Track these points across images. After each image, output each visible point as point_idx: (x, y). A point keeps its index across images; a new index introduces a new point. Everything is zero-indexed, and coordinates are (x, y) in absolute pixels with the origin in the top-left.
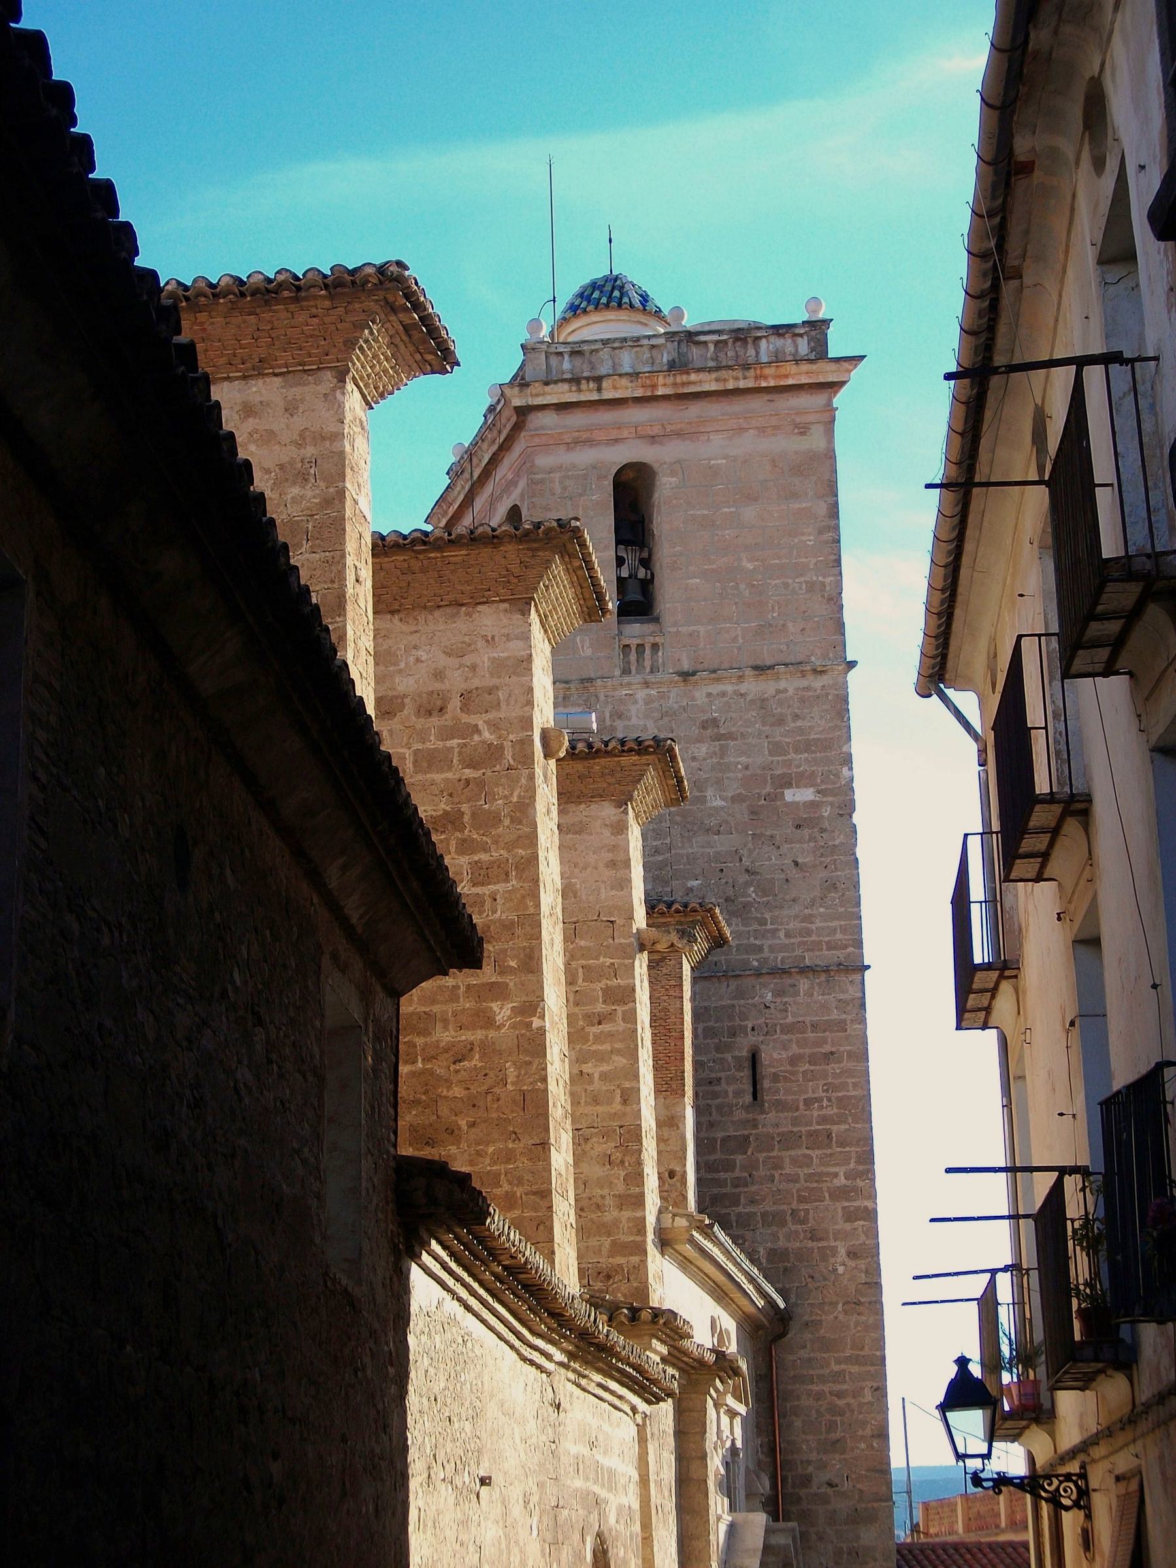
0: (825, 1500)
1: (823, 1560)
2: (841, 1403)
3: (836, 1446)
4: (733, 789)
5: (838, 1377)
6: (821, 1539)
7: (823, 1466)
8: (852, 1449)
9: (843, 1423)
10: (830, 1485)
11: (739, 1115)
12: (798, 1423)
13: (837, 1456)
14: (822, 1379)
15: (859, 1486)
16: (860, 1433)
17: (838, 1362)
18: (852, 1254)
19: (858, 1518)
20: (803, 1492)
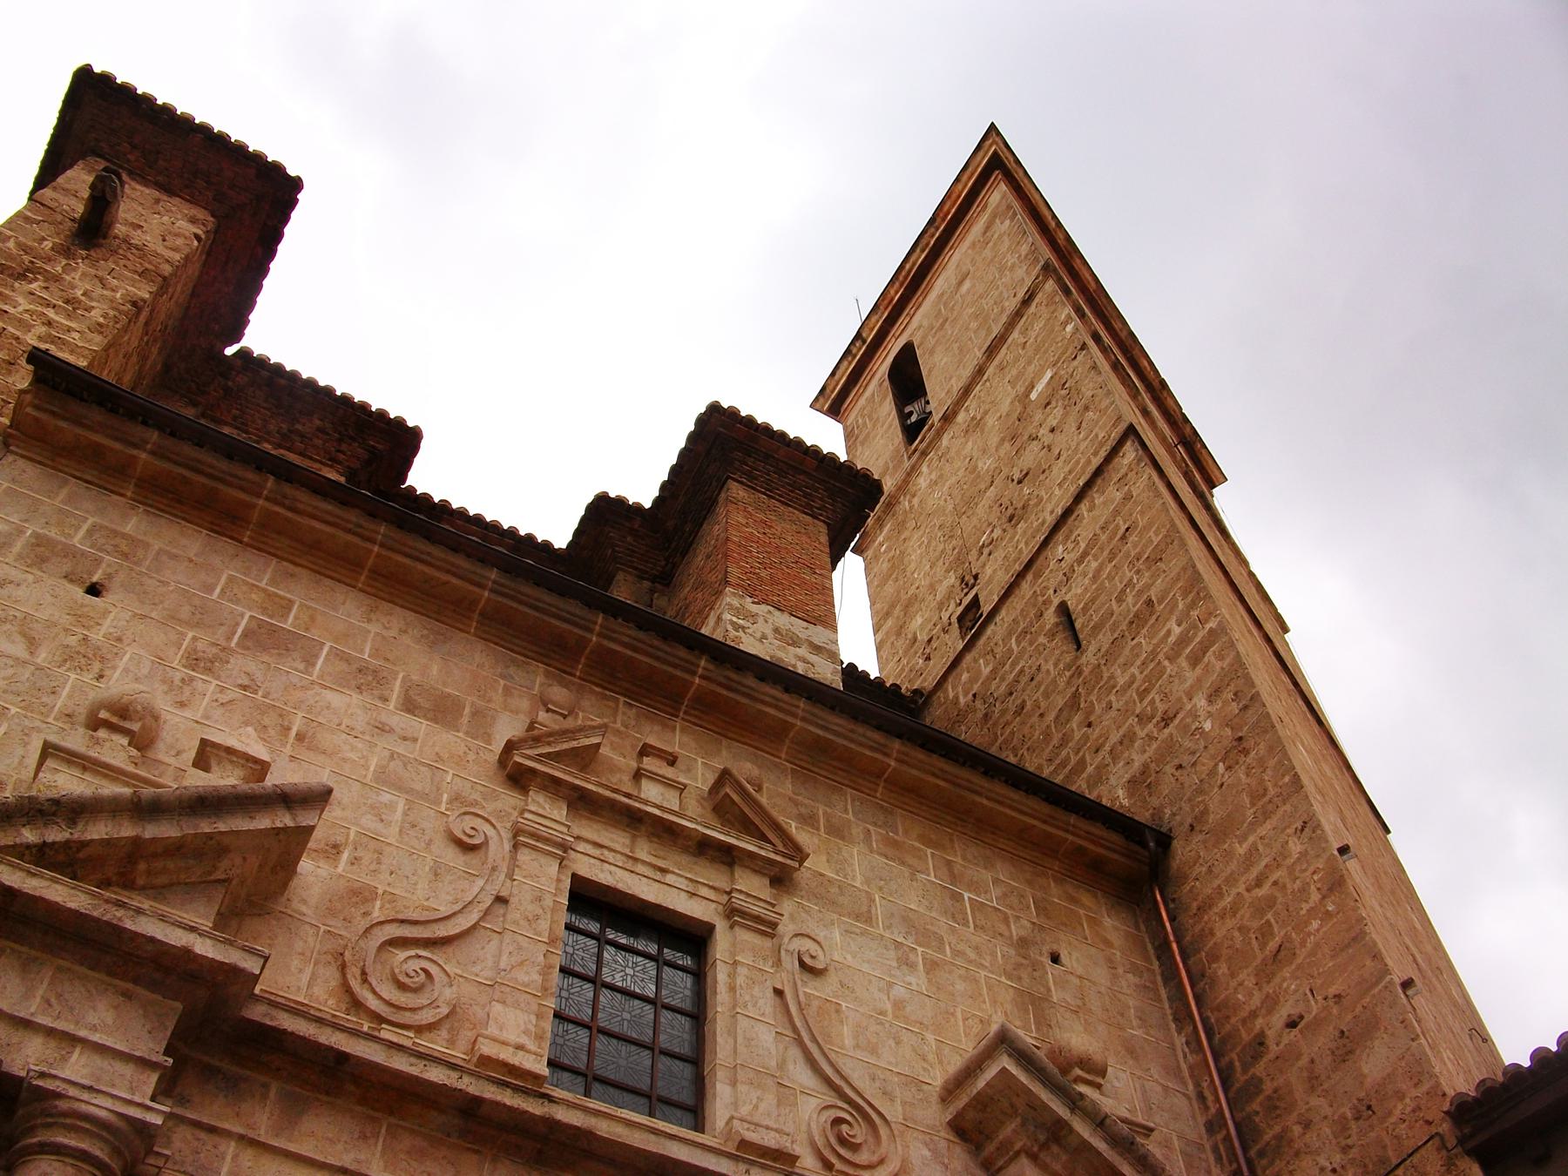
0: (1292, 1054)
1: (1323, 1162)
3: (1279, 956)
4: (994, 440)
5: (1251, 856)
6: (1307, 1125)
7: (1271, 1003)
8: (1303, 943)
9: (1277, 914)
10: (1292, 1024)
13: (1286, 972)
14: (1231, 880)
15: (1332, 991)
16: (1305, 907)
19: (1347, 1047)
20: (1259, 1069)
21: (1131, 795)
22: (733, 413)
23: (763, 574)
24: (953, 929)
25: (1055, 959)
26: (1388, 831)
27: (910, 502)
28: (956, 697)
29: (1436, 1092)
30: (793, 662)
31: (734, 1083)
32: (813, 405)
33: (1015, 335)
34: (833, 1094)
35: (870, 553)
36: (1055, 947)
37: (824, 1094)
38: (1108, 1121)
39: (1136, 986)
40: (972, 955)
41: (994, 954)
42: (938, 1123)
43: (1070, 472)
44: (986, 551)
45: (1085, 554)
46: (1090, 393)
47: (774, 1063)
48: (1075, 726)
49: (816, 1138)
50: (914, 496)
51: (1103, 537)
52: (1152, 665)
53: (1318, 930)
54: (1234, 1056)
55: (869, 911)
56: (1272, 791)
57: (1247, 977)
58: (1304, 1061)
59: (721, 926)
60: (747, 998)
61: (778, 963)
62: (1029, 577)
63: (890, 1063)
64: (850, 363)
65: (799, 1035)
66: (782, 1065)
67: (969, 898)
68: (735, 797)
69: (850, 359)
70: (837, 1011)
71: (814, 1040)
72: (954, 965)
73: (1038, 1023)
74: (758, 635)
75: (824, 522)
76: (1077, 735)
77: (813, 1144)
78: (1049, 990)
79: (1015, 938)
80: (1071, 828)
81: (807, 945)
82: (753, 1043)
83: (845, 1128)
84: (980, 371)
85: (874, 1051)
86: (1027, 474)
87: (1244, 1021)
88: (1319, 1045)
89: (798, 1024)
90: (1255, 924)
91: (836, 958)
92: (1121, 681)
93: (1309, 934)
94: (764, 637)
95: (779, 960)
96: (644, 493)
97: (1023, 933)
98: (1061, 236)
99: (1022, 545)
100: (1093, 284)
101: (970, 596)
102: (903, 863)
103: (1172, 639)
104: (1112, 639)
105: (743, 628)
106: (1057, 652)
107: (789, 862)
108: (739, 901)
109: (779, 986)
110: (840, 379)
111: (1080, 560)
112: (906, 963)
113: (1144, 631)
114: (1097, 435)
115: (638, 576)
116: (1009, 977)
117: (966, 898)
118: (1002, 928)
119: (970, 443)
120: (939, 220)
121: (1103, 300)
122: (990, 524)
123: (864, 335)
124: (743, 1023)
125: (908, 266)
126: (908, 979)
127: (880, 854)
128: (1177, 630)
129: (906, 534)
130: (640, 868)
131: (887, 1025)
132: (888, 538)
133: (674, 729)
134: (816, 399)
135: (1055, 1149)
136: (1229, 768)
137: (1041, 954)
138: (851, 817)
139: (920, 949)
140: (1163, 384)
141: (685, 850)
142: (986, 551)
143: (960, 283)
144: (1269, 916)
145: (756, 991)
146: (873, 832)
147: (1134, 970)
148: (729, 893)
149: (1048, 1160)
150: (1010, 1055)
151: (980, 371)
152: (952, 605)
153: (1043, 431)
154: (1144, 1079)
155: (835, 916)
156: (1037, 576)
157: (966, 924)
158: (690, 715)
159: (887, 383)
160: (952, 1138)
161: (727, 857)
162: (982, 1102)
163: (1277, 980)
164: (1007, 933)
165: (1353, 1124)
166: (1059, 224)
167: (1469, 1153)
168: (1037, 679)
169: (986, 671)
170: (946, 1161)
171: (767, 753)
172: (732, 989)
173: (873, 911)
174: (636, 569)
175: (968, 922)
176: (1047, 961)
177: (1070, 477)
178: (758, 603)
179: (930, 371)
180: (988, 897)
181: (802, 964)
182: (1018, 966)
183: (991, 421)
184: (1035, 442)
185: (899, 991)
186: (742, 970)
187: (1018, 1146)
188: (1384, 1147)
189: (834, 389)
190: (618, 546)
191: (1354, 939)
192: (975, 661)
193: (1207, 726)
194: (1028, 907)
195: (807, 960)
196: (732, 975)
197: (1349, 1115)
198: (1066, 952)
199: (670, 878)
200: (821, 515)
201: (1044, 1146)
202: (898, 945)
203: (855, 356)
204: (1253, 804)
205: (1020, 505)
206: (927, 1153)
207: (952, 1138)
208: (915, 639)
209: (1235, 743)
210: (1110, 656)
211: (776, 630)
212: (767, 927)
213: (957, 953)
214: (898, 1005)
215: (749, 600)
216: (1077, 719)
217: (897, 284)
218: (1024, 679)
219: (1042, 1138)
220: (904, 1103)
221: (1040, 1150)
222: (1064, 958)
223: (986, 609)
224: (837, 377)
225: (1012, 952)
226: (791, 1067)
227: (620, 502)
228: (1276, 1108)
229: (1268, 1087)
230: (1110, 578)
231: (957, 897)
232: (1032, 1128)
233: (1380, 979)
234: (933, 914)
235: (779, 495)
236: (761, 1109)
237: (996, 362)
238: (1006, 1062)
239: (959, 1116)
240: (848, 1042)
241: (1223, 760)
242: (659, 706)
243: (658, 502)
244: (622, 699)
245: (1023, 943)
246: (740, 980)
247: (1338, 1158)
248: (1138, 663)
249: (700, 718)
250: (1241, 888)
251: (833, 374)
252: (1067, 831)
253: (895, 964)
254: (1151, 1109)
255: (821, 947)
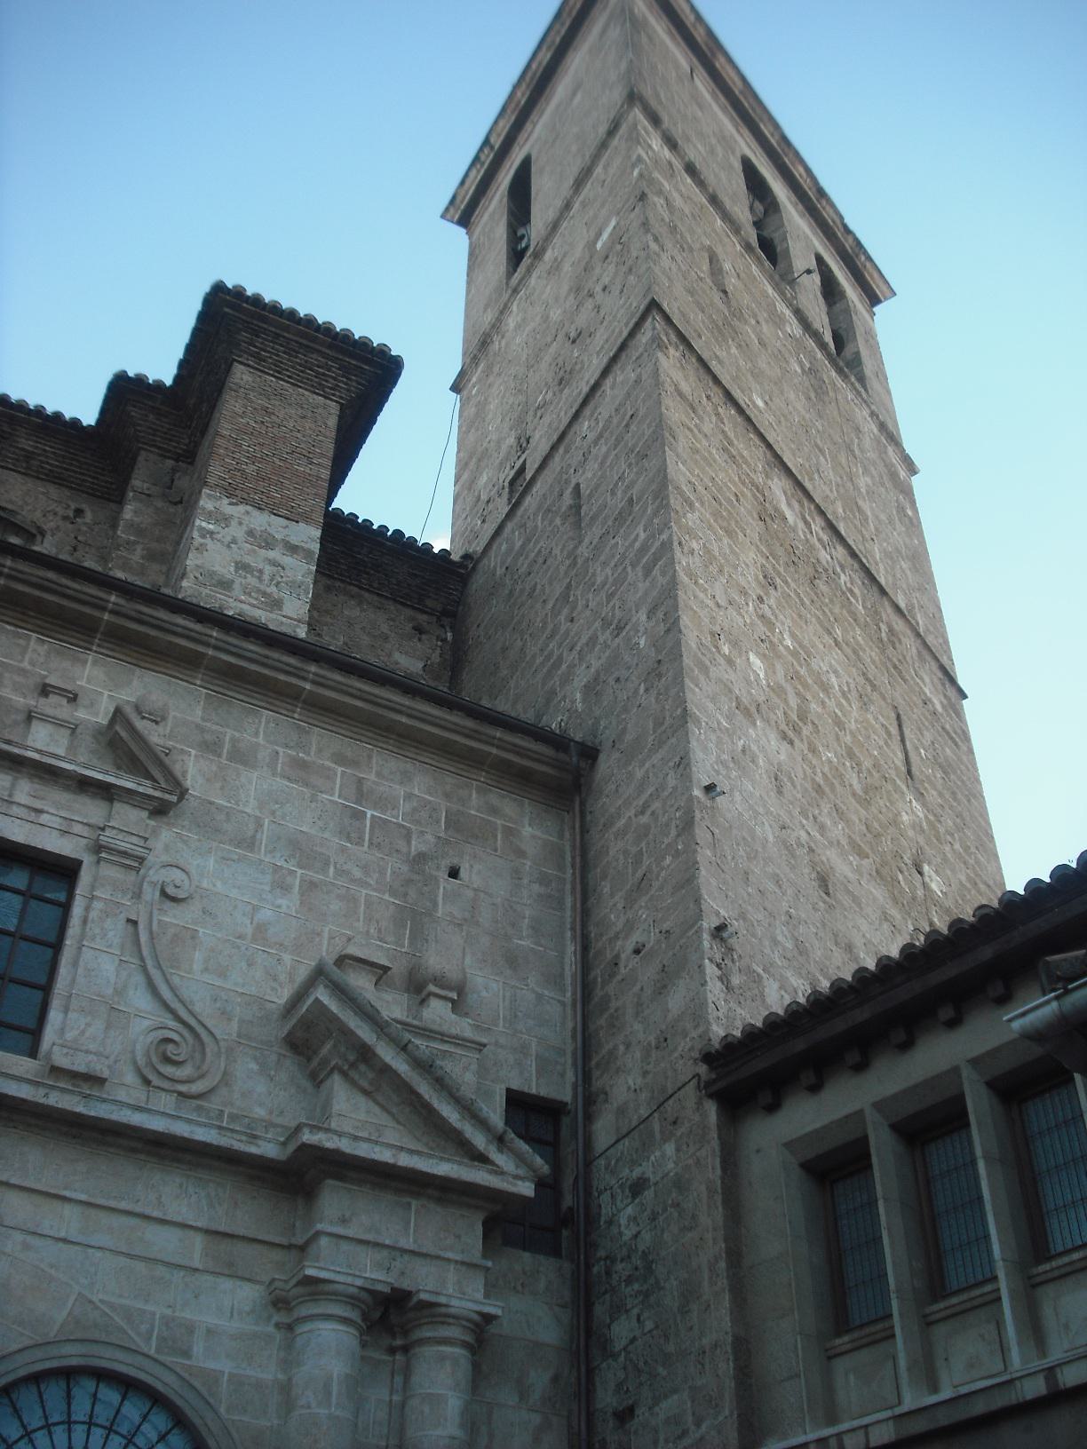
2: (644, 819)
4: (565, 288)
7: (630, 926)
8: (657, 879)
11: (563, 569)
12: (607, 890)
15: (666, 926)
16: (666, 841)
17: (642, 764)
18: (651, 614)
20: (611, 989)
21: (584, 701)
22: (239, 293)
23: (250, 469)
24: (343, 850)
25: (454, 873)
26: (965, 696)
27: (500, 342)
28: (495, 568)
29: (705, 1036)
30: (261, 567)
31: (66, 1010)
32: (443, 216)
33: (599, 170)
34: (170, 1016)
35: (465, 393)
36: (455, 861)
37: (159, 1016)
38: (410, 1046)
39: (540, 895)
40: (357, 873)
41: (382, 872)
42: (273, 1039)
43: (607, 341)
44: (539, 415)
45: (600, 436)
46: (635, 254)
47: (110, 991)
48: (563, 618)
49: (138, 1058)
50: (503, 337)
51: (615, 421)
52: (620, 570)
53: (669, 866)
54: (599, 971)
55: (254, 837)
56: (668, 721)
57: (619, 899)
58: (637, 988)
59: (87, 860)
60: (97, 931)
61: (138, 895)
62: (561, 450)
63: (236, 984)
64: (478, 171)
65: (144, 962)
66: (120, 992)
67: (373, 816)
68: (123, 734)
69: (478, 166)
70: (193, 938)
71: (159, 967)
72: (333, 884)
73: (413, 938)
74: (229, 539)
75: (336, 402)
76: (563, 628)
77: (135, 1063)
78: (435, 904)
79: (413, 852)
80: (496, 742)
81: (177, 875)
82: (93, 973)
83: (170, 1048)
84: (567, 206)
85: (223, 974)
86: (580, 333)
87: (610, 940)
88: (648, 974)
89: (146, 952)
90: (634, 850)
91: (205, 885)
92: (599, 580)
93: (662, 869)
94: (234, 541)
95: (141, 892)
96: (162, 367)
97: (423, 848)
98: (702, 31)
99: (562, 413)
100: (739, 83)
101: (521, 460)
102: (307, 785)
103: (637, 545)
104: (601, 532)
105: (212, 533)
106: (565, 537)
107: (167, 796)
108: (107, 837)
109: (134, 918)
110: (469, 188)
111: (596, 442)
112: (282, 887)
113: (622, 531)
114: (631, 304)
115: (161, 455)
116: (393, 893)
117: (369, 816)
118: (401, 844)
119: (549, 287)
120: (565, 15)
121: (751, 100)
122: (546, 384)
123: (492, 140)
124: (87, 954)
125: (534, 66)
126: (279, 901)
127: (283, 777)
128: (642, 536)
129: (491, 379)
130: (15, 810)
131: (243, 948)
132: (479, 380)
133: (86, 662)
134: (447, 209)
135: (363, 1067)
136: (647, 690)
137: (438, 868)
138: (261, 740)
139: (300, 871)
140: (821, 193)
141: (67, 788)
142: (539, 415)
143: (574, 94)
144: (643, 844)
145: (109, 923)
146: (281, 754)
147: (543, 880)
148: (103, 829)
149: (356, 1077)
150: (326, 986)
151: (567, 206)
152: (508, 468)
153: (598, 289)
154: (517, 988)
155: (215, 844)
156: (567, 451)
157: (360, 842)
158: (103, 647)
159: (505, 200)
160: (284, 1052)
161: (106, 792)
162: (306, 1024)
163: (636, 907)
164: (405, 850)
165: (654, 1053)
166: (699, 18)
167: (710, 1096)
168: (548, 563)
169: (518, 544)
170: (273, 1073)
171: (181, 680)
172: (85, 921)
173: (258, 836)
174: (159, 448)
175: (364, 840)
176: (443, 875)
177: (606, 346)
178: (236, 504)
179: (537, 194)
180: (395, 812)
181: (164, 894)
182: (409, 882)
183: (567, 267)
184: (590, 300)
185: (266, 914)
186: (97, 905)
187: (333, 1063)
188: (667, 1078)
189: (464, 197)
190: (140, 425)
191: (688, 880)
192: (513, 532)
193: (642, 642)
194: (438, 821)
195: (170, 891)
196: (87, 909)
197: (653, 1044)
198: (467, 866)
199: (44, 818)
200: (334, 395)
201: (353, 1065)
202: (277, 869)
203: (483, 164)
204: (654, 732)
205: (568, 370)
206: (254, 1066)
207: (284, 1052)
208: (479, 499)
209: (656, 665)
210: (597, 550)
211: (250, 533)
212: (135, 861)
213: (341, 873)
214: (261, 930)
215: (226, 501)
216: (565, 611)
217: (524, 86)
218: (541, 560)
219: (352, 1058)
220: (242, 1021)
221: (349, 1069)
222: (463, 873)
223: (529, 475)
224: (467, 185)
225: (405, 868)
226: (131, 993)
227: (140, 380)
228: (614, 1026)
229: (613, 1005)
230: (611, 467)
231: (359, 816)
232: (343, 1049)
233: (693, 925)
234: (327, 835)
235: (289, 377)
236: (87, 1034)
237: (581, 198)
238: (322, 994)
239: (290, 1033)
240: (197, 967)
241: (645, 681)
242: (71, 640)
243: (178, 379)
244: (34, 635)
245: (421, 858)
246: (93, 915)
247: (639, 1081)
248: (613, 564)
249: (112, 650)
250: (632, 813)
251: (463, 183)
252: (493, 745)
253: (267, 888)
254: (516, 1016)
255: (189, 877)
